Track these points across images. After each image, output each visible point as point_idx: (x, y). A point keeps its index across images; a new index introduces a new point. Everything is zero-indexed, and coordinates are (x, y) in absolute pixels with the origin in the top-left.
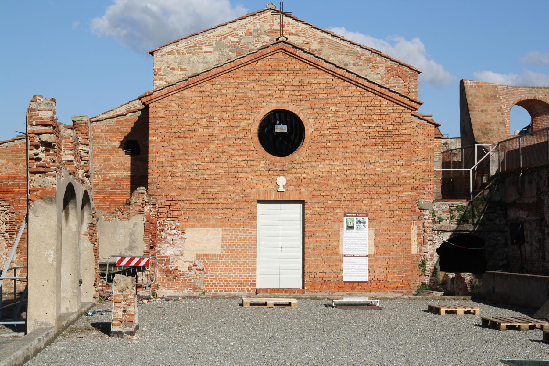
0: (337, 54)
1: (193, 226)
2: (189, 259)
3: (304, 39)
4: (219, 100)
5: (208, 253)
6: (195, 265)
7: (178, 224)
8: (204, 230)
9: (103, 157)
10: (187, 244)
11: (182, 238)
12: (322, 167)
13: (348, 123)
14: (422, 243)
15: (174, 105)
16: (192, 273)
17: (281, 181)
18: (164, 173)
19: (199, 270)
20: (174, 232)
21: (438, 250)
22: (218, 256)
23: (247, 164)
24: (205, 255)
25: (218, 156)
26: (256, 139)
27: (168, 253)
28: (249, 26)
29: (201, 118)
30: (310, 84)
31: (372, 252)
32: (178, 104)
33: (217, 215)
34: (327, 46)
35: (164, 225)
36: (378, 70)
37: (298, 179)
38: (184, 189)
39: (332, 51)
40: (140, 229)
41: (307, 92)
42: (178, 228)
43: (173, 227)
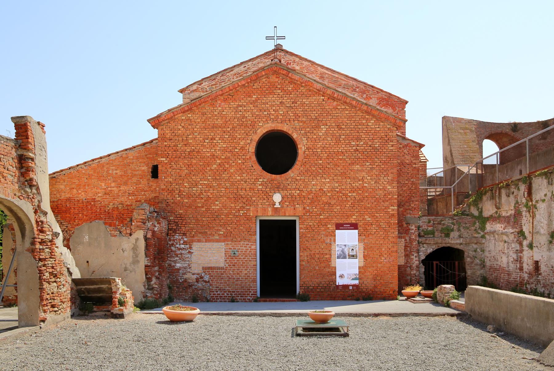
1: (199, 241)
2: (196, 272)
5: (213, 265)
6: (202, 277)
7: (185, 239)
8: (208, 245)
9: (134, 180)
10: (194, 258)
11: (189, 252)
16: (200, 285)
18: (171, 192)
19: (206, 282)
20: (182, 246)
22: (222, 268)
23: (246, 182)
24: (211, 268)
25: (220, 175)
27: (178, 265)
33: (220, 230)
35: (174, 240)
38: (190, 207)
40: (142, 244)
42: (185, 243)
43: (182, 242)
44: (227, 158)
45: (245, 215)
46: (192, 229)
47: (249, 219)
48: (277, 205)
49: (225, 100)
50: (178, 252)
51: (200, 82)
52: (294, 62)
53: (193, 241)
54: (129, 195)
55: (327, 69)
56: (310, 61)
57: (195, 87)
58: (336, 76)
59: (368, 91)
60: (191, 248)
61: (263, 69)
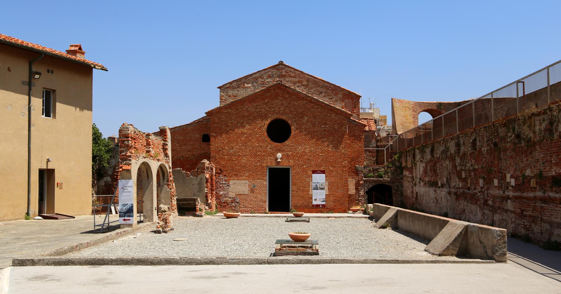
1: (233, 179)
2: (232, 196)
4: (246, 114)
12: (300, 149)
13: (314, 125)
14: (357, 189)
17: (279, 155)
19: (237, 202)
20: (224, 182)
22: (247, 195)
25: (246, 143)
26: (266, 134)
28: (270, 73)
29: (237, 123)
30: (294, 105)
31: (327, 193)
37: (288, 156)
39: (313, 86)
41: (292, 109)
42: (226, 180)
44: (250, 134)
45: (260, 165)
47: (263, 167)
48: (279, 160)
49: (250, 102)
51: (231, 83)
53: (230, 179)
54: (188, 151)
55: (311, 76)
57: (228, 86)
59: (337, 90)
60: (229, 183)
61: (272, 86)
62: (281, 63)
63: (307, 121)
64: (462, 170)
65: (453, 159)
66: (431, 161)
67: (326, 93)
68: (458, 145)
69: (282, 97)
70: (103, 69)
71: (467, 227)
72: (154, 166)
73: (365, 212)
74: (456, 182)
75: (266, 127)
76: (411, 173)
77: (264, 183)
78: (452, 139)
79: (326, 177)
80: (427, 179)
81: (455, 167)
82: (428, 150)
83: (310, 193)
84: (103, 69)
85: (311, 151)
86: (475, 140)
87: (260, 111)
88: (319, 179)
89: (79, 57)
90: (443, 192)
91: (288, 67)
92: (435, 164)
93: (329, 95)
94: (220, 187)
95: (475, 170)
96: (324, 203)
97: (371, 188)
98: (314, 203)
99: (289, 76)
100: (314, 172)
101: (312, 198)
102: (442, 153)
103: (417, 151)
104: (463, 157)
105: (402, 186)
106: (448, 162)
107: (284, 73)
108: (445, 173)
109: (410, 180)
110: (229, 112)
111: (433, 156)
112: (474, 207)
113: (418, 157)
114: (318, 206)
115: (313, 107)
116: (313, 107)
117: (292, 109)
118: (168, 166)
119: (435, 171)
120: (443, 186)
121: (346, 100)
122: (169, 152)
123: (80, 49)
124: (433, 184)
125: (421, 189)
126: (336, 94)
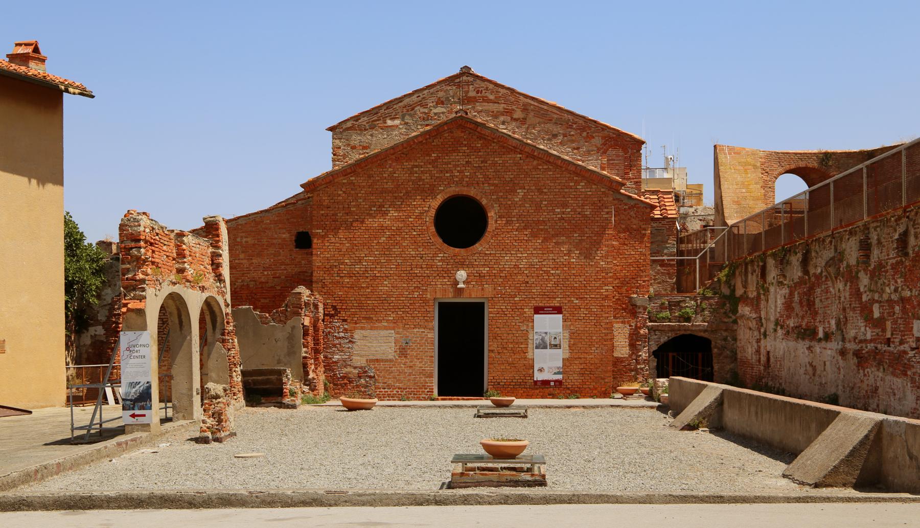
0: (545, 123)
1: (362, 328)
2: (358, 364)
3: (505, 106)
4: (390, 185)
9: (272, 250)
12: (508, 261)
13: (538, 208)
14: (632, 346)
15: (340, 192)
17: (462, 275)
19: (370, 377)
20: (342, 335)
21: (655, 354)
22: (391, 361)
25: (389, 249)
26: (433, 229)
28: (441, 94)
29: (370, 207)
30: (494, 164)
31: (567, 356)
32: (344, 192)
34: (532, 114)
36: (593, 141)
37: (481, 276)
39: (538, 120)
41: (490, 172)
42: (346, 330)
44: (399, 229)
46: (354, 314)
47: (426, 301)
48: (461, 285)
49: (397, 160)
50: (337, 342)
51: (356, 118)
52: (487, 89)
53: (355, 328)
54: (265, 269)
55: (533, 99)
56: (509, 89)
57: (349, 124)
58: (545, 107)
59: (590, 128)
60: (352, 337)
62: (466, 71)
63: (524, 199)
64: (873, 301)
65: (851, 277)
66: (802, 282)
67: (565, 135)
68: (865, 247)
69: (469, 146)
70: (84, 93)
71: (880, 425)
72: (194, 301)
73: (650, 396)
74: (858, 329)
75: (433, 213)
76: (757, 308)
77: (429, 336)
78: (851, 233)
79: (565, 320)
80: (791, 323)
81: (857, 294)
82: (795, 260)
83: (529, 355)
84: (84, 93)
85: (531, 265)
86: (905, 234)
87: (420, 179)
88: (549, 325)
89: (34, 69)
90: (828, 352)
91: (482, 79)
92: (812, 289)
93: (573, 141)
94: (335, 346)
95: (903, 300)
96: (560, 377)
97: (665, 344)
98: (538, 376)
99: (484, 101)
100: (538, 310)
101: (533, 366)
102: (828, 265)
103: (771, 262)
104: (877, 273)
105: (735, 339)
106: (840, 285)
107: (472, 94)
108: (834, 310)
109: (753, 324)
110: (351, 183)
111: (806, 272)
112: (898, 382)
113: (773, 274)
114: (546, 383)
115: (536, 168)
116: (536, 168)
117: (490, 172)
118: (223, 300)
119: (811, 304)
120: (827, 337)
121: (611, 152)
122: (226, 271)
123: (36, 50)
124: (807, 334)
125: (778, 345)
126: (589, 138)
